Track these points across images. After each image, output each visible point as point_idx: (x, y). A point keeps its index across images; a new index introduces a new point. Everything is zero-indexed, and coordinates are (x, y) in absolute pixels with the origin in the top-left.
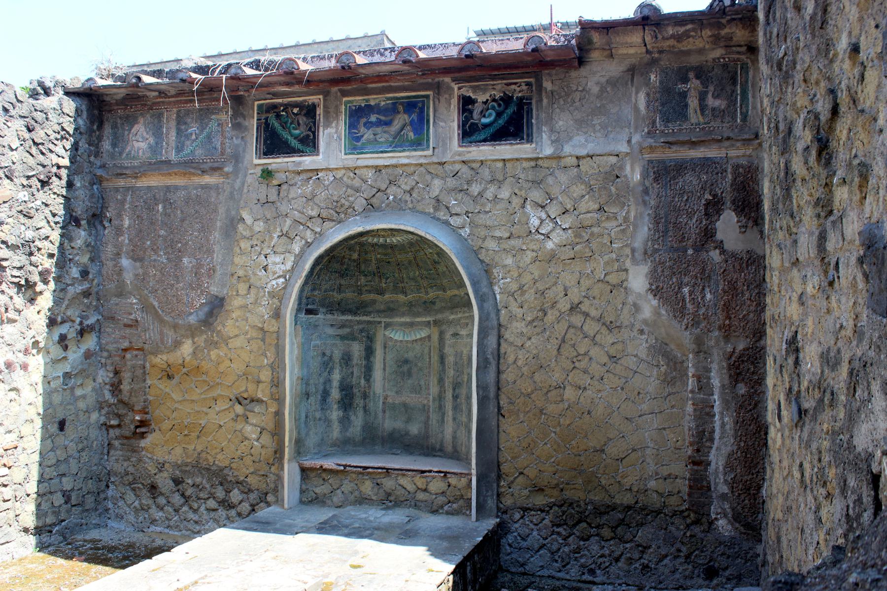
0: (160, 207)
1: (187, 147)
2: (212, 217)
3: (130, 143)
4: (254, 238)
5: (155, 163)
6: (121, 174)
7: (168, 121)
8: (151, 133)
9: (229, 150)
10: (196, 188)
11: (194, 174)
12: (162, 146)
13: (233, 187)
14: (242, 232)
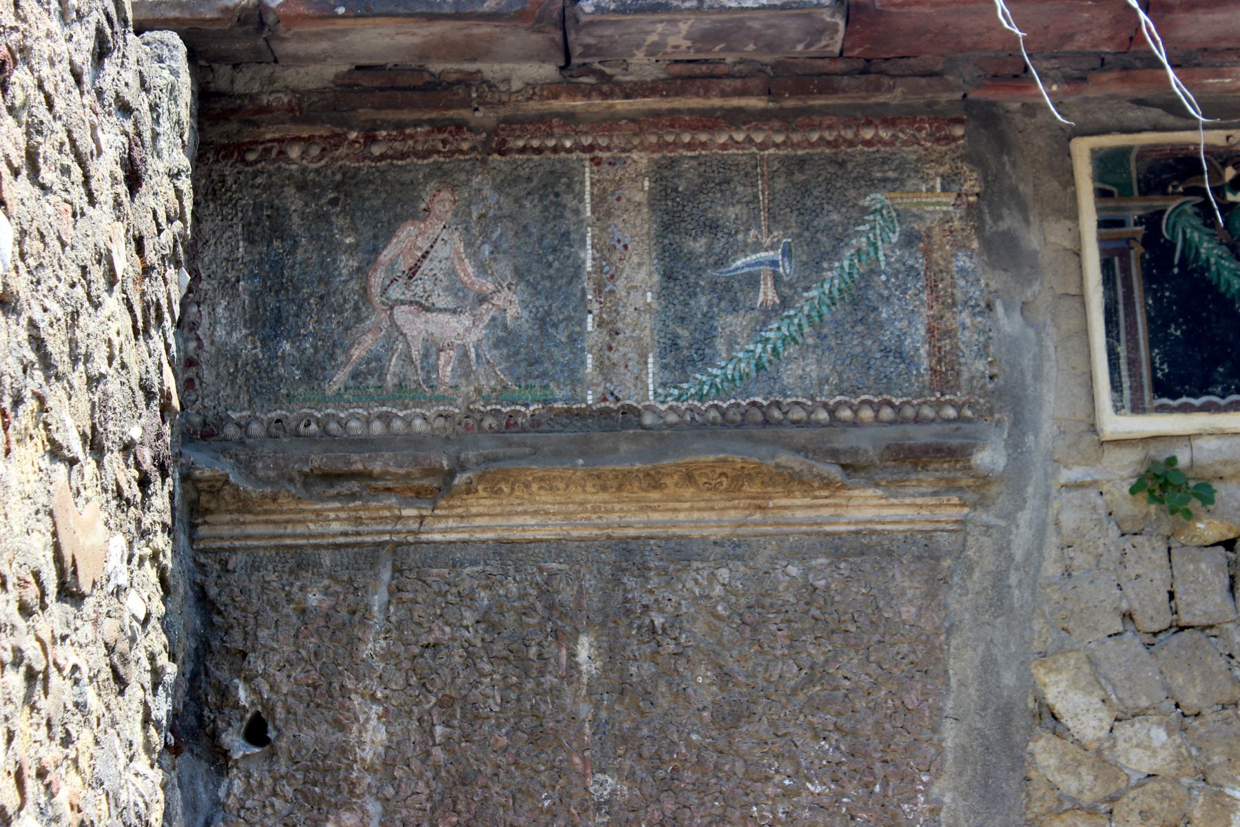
0: (584, 649)
1: (731, 343)
2: (912, 700)
3: (379, 318)
4: (1120, 808)
5: (535, 423)
6: (330, 477)
7: (603, 210)
8: (504, 267)
9: (980, 365)
10: (798, 554)
11: (792, 480)
12: (572, 339)
13: (1003, 549)
14: (1057, 778)
